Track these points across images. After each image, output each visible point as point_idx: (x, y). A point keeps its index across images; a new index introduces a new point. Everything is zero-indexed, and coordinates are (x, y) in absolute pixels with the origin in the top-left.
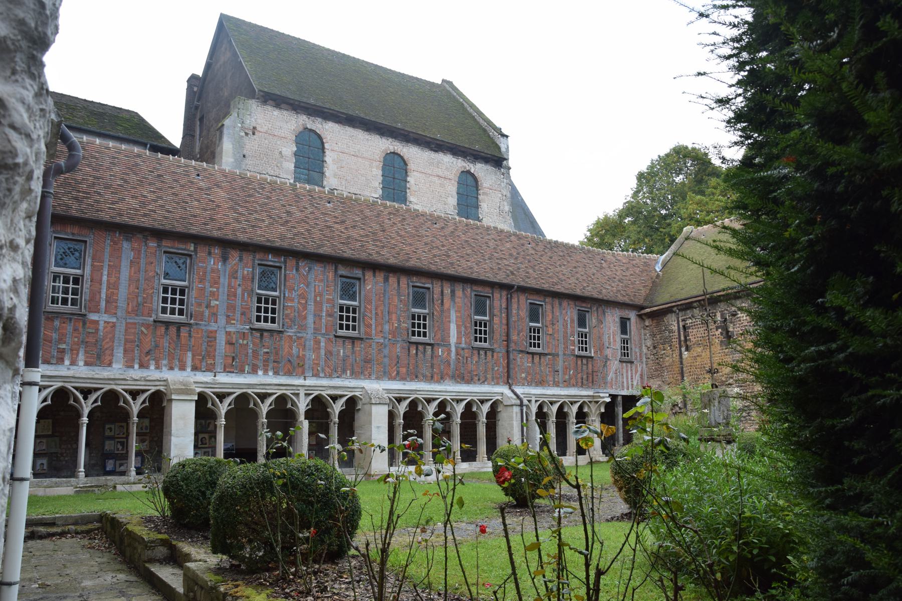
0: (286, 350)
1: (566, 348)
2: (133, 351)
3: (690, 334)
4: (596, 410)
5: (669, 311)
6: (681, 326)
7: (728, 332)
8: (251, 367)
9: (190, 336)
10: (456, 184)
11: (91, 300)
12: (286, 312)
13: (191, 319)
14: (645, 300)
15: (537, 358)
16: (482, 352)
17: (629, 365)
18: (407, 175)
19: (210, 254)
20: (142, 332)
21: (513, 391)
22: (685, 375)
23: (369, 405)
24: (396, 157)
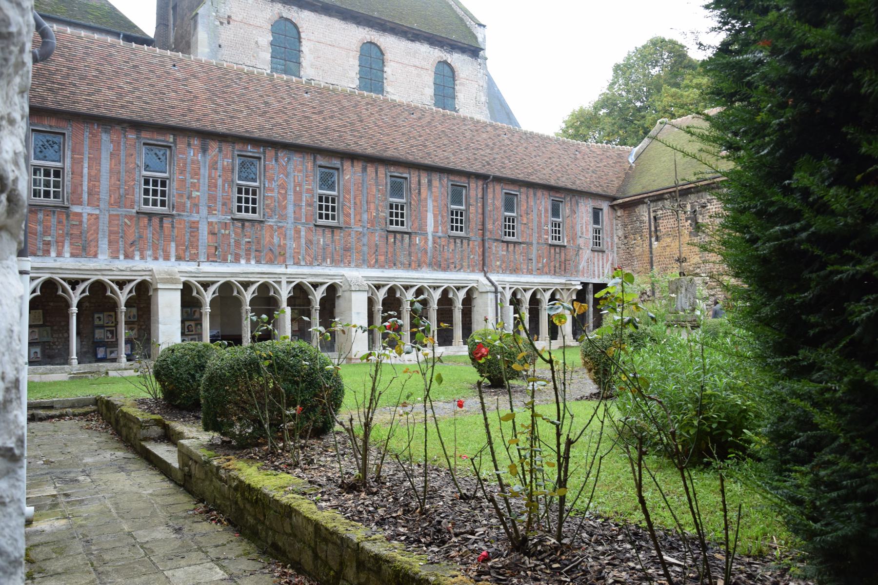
0: (268, 239)
1: (540, 237)
2: (118, 242)
3: (661, 225)
4: (568, 298)
5: (641, 202)
6: (652, 217)
7: (697, 223)
8: (233, 256)
9: (173, 227)
10: (433, 74)
11: (73, 193)
12: (266, 202)
13: (173, 210)
14: (618, 191)
15: (511, 247)
16: (458, 241)
17: (600, 254)
18: (383, 65)
19: (189, 145)
20: (126, 223)
21: (488, 279)
23: (349, 292)
24: (373, 46)
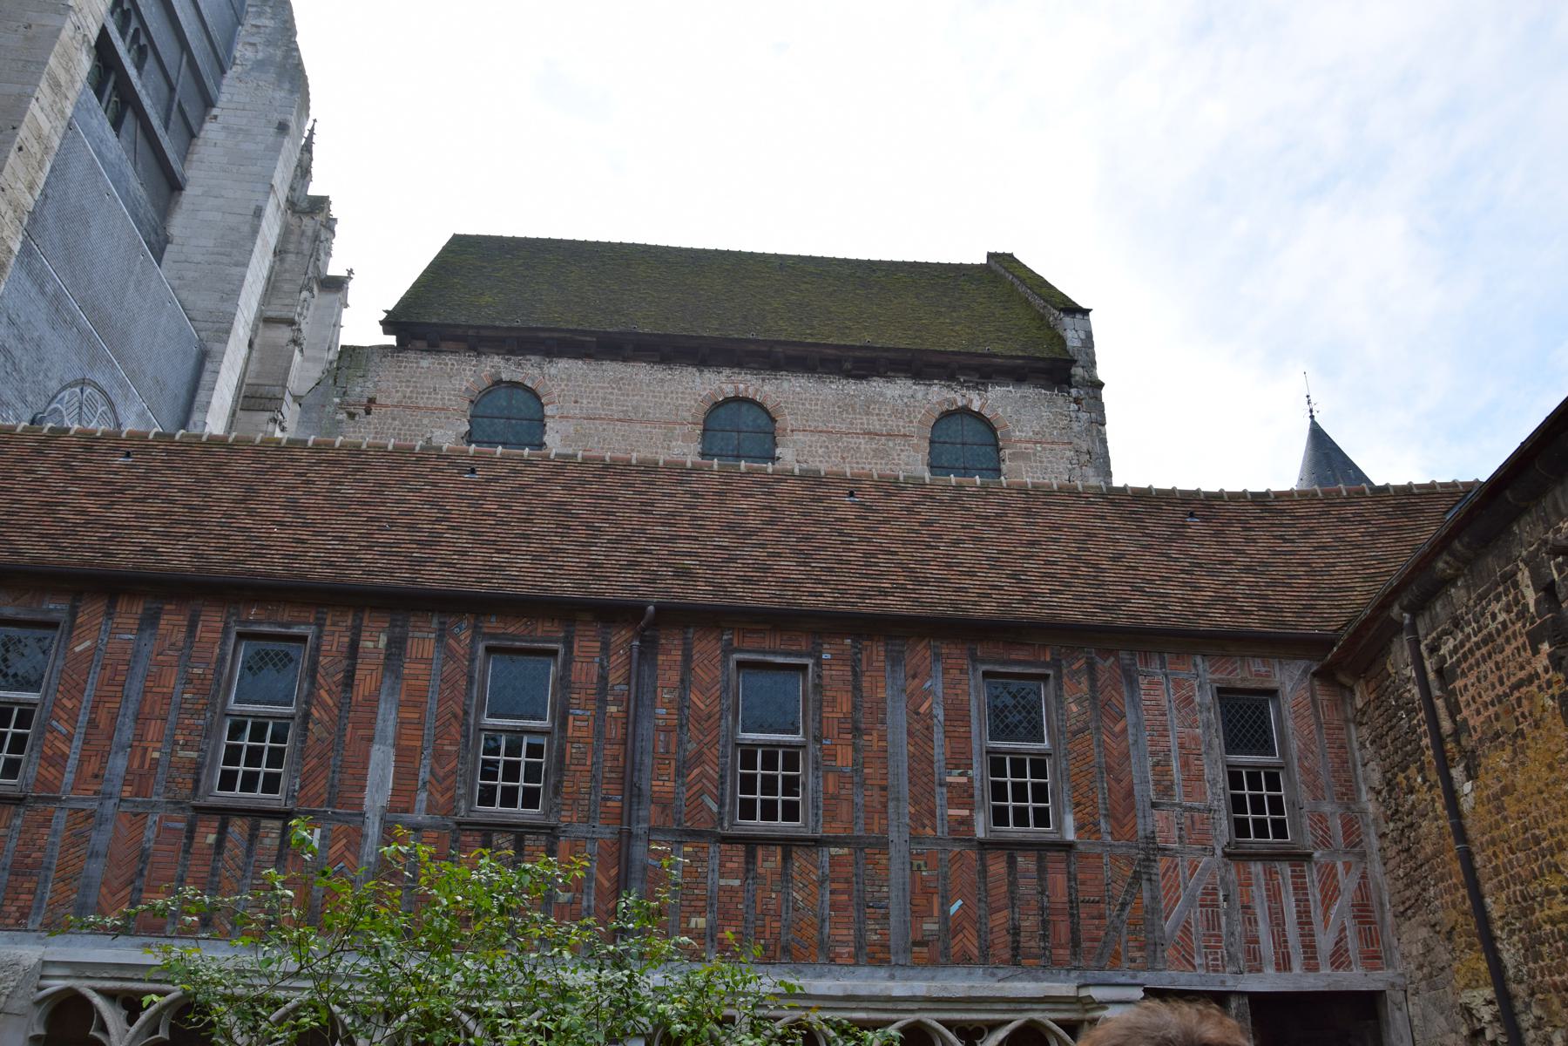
3: (1462, 700)
6: (1431, 676)
10: (926, 444)
15: (769, 862)
17: (1286, 869)
22: (1487, 887)
24: (745, 407)
